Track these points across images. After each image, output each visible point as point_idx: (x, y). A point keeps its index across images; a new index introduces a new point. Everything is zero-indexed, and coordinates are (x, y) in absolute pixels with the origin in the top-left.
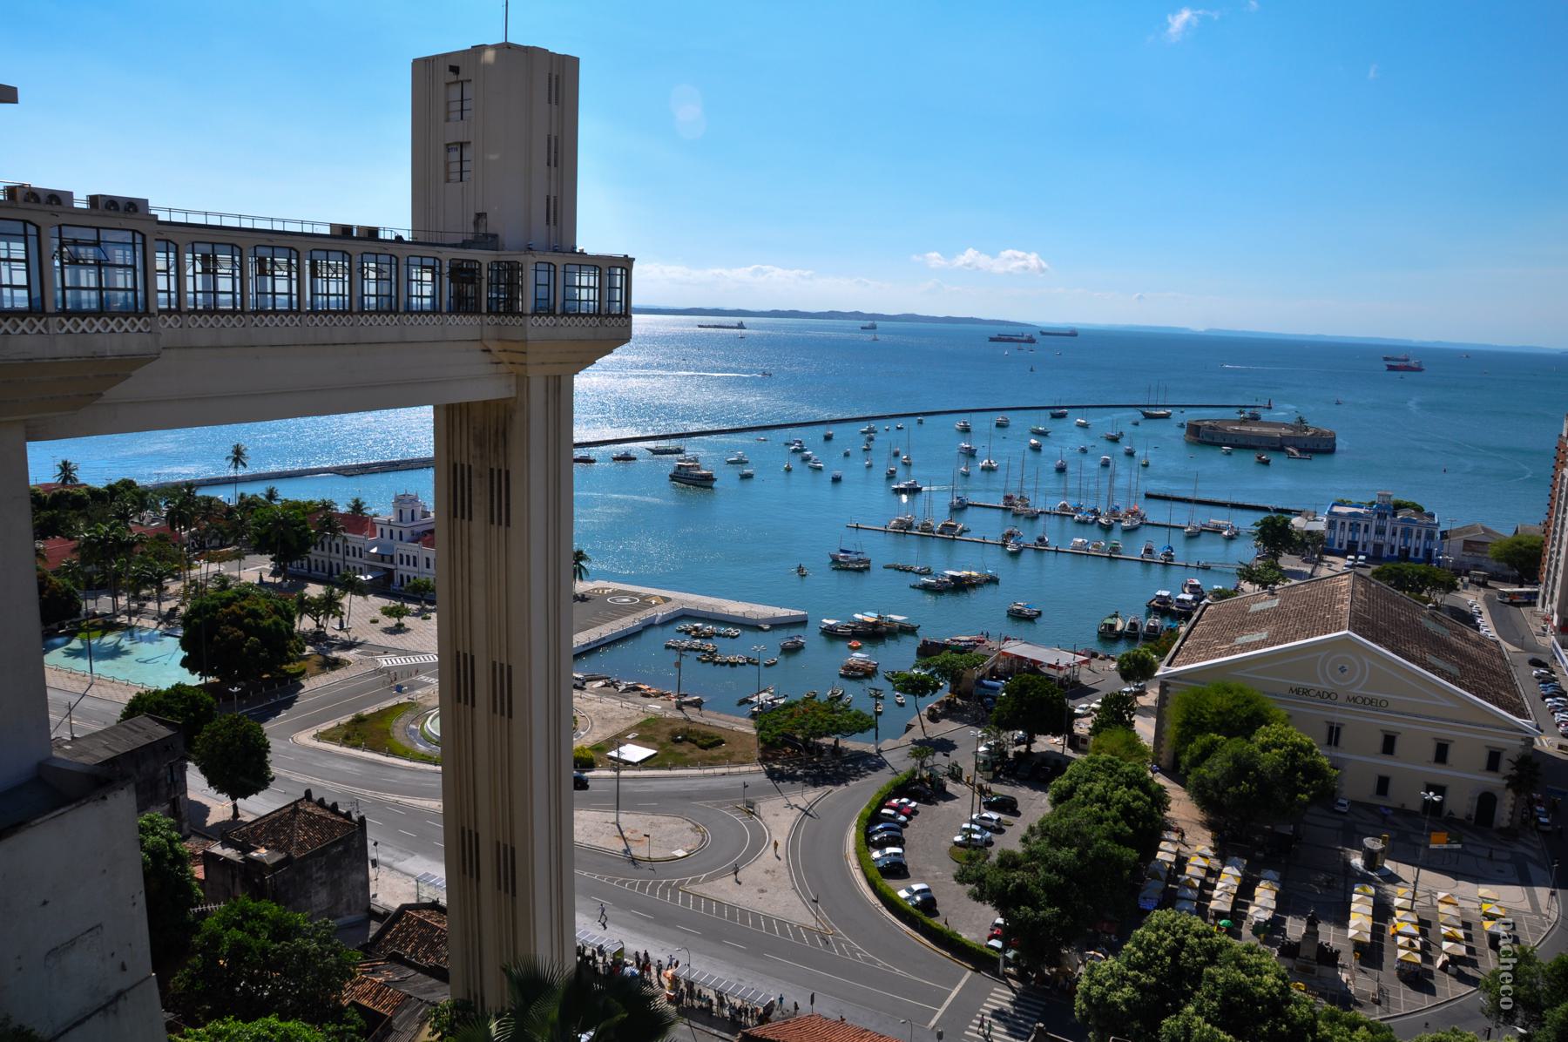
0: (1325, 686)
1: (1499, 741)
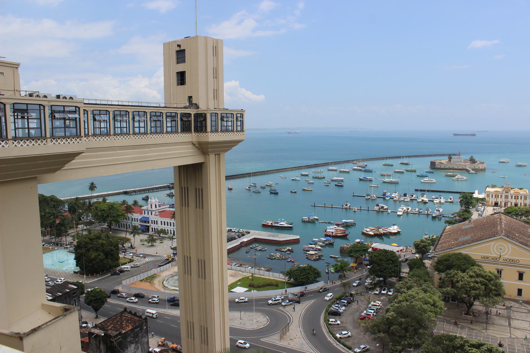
0: (494, 255)
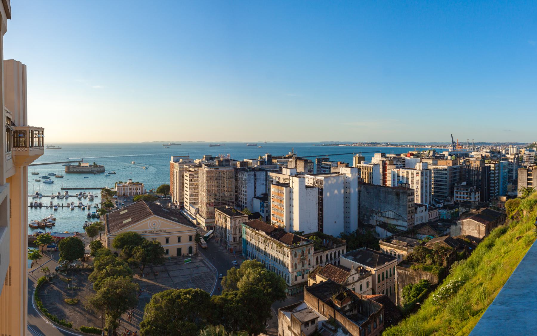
0: (150, 230)
1: (191, 234)
